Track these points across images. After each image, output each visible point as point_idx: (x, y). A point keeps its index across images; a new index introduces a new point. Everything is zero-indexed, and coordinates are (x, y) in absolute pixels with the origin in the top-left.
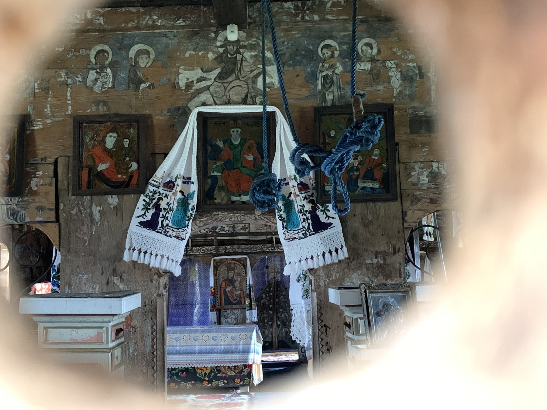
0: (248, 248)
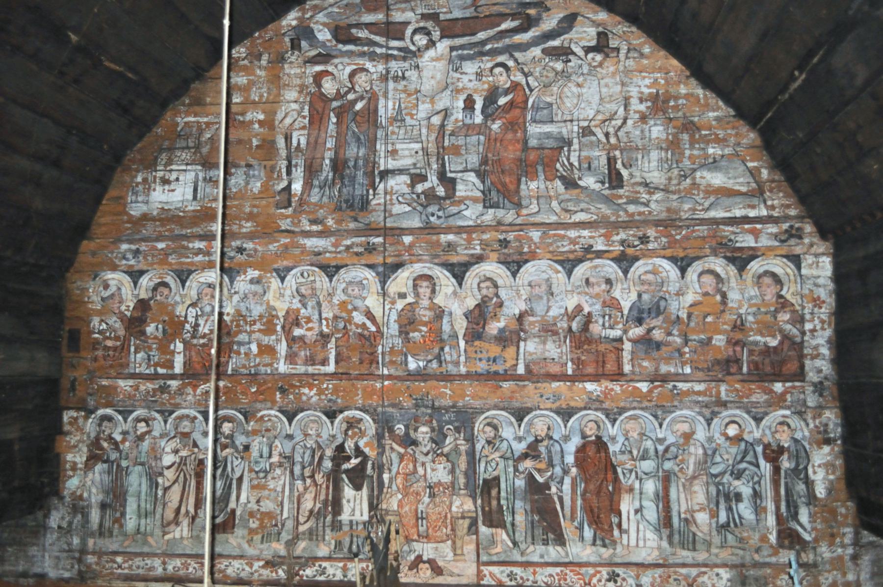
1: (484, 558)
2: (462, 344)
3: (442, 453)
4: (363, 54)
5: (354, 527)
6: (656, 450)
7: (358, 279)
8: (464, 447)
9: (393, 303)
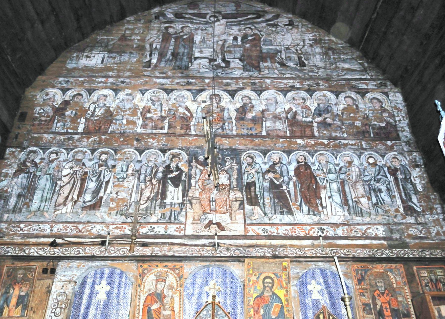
0: (181, 251)
1: (248, 222)
2: (234, 122)
3: (224, 169)
4: (188, 22)
5: (173, 206)
6: (336, 170)
7: (182, 95)
8: (236, 167)
9: (199, 104)
